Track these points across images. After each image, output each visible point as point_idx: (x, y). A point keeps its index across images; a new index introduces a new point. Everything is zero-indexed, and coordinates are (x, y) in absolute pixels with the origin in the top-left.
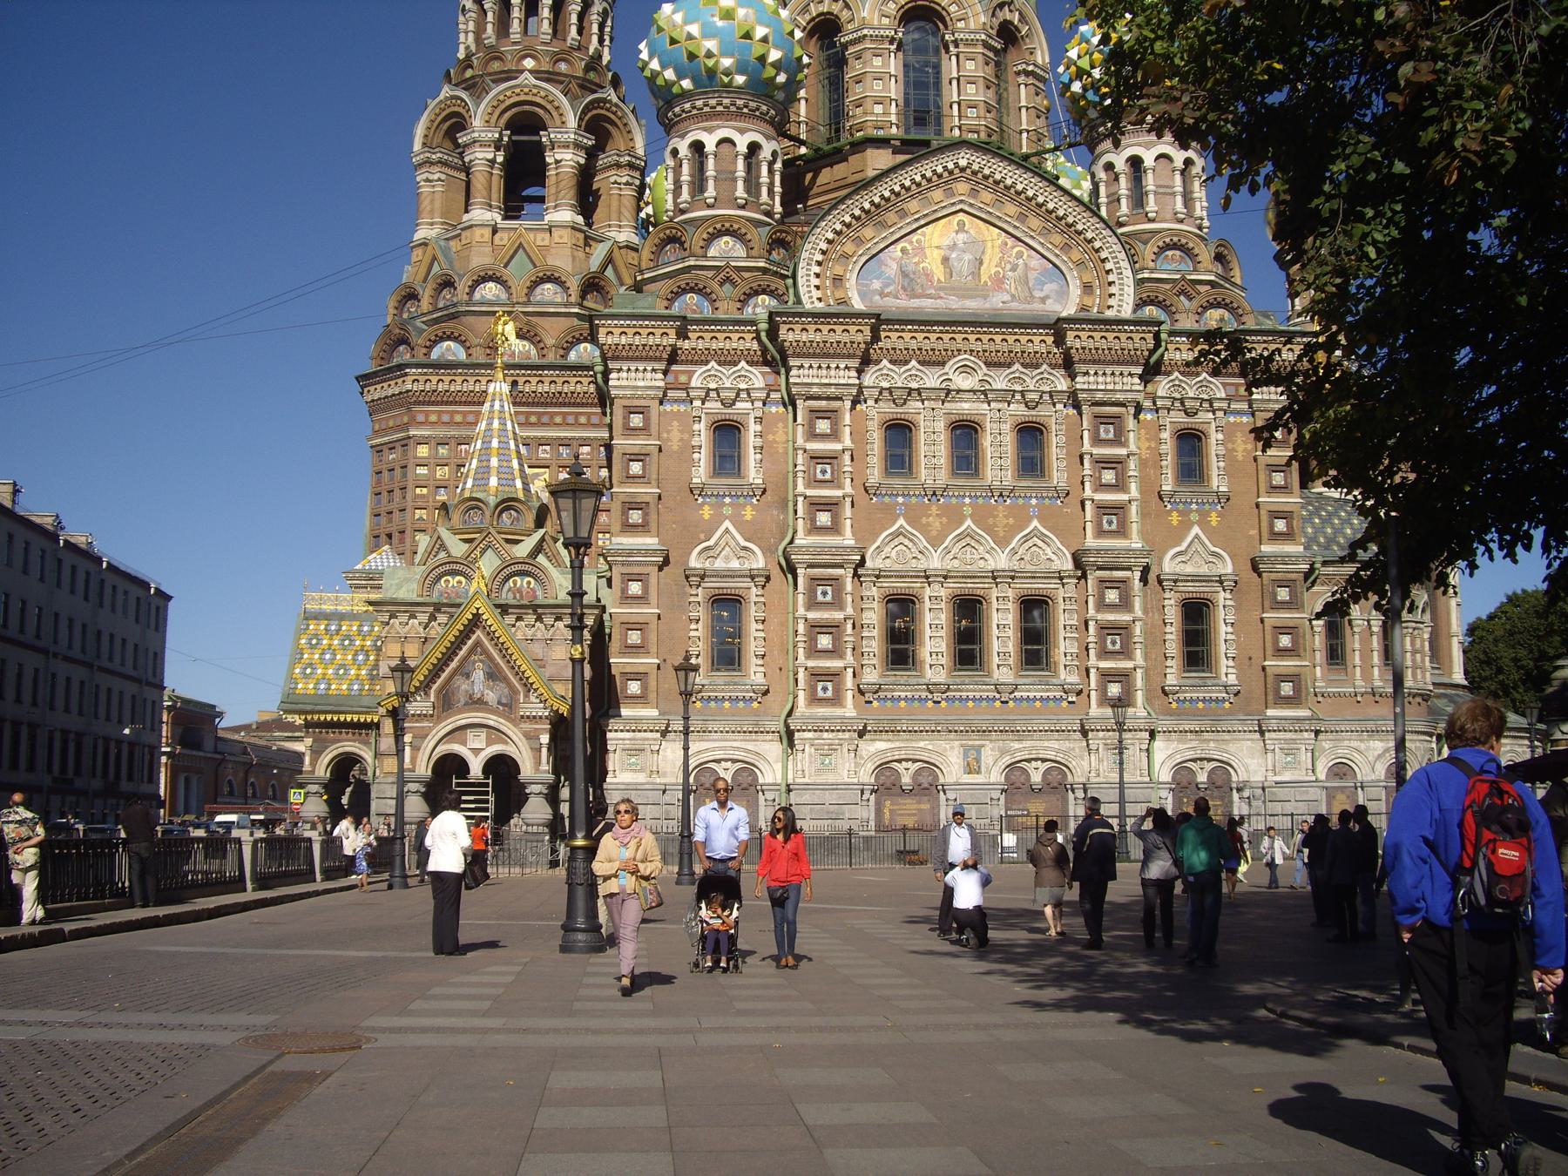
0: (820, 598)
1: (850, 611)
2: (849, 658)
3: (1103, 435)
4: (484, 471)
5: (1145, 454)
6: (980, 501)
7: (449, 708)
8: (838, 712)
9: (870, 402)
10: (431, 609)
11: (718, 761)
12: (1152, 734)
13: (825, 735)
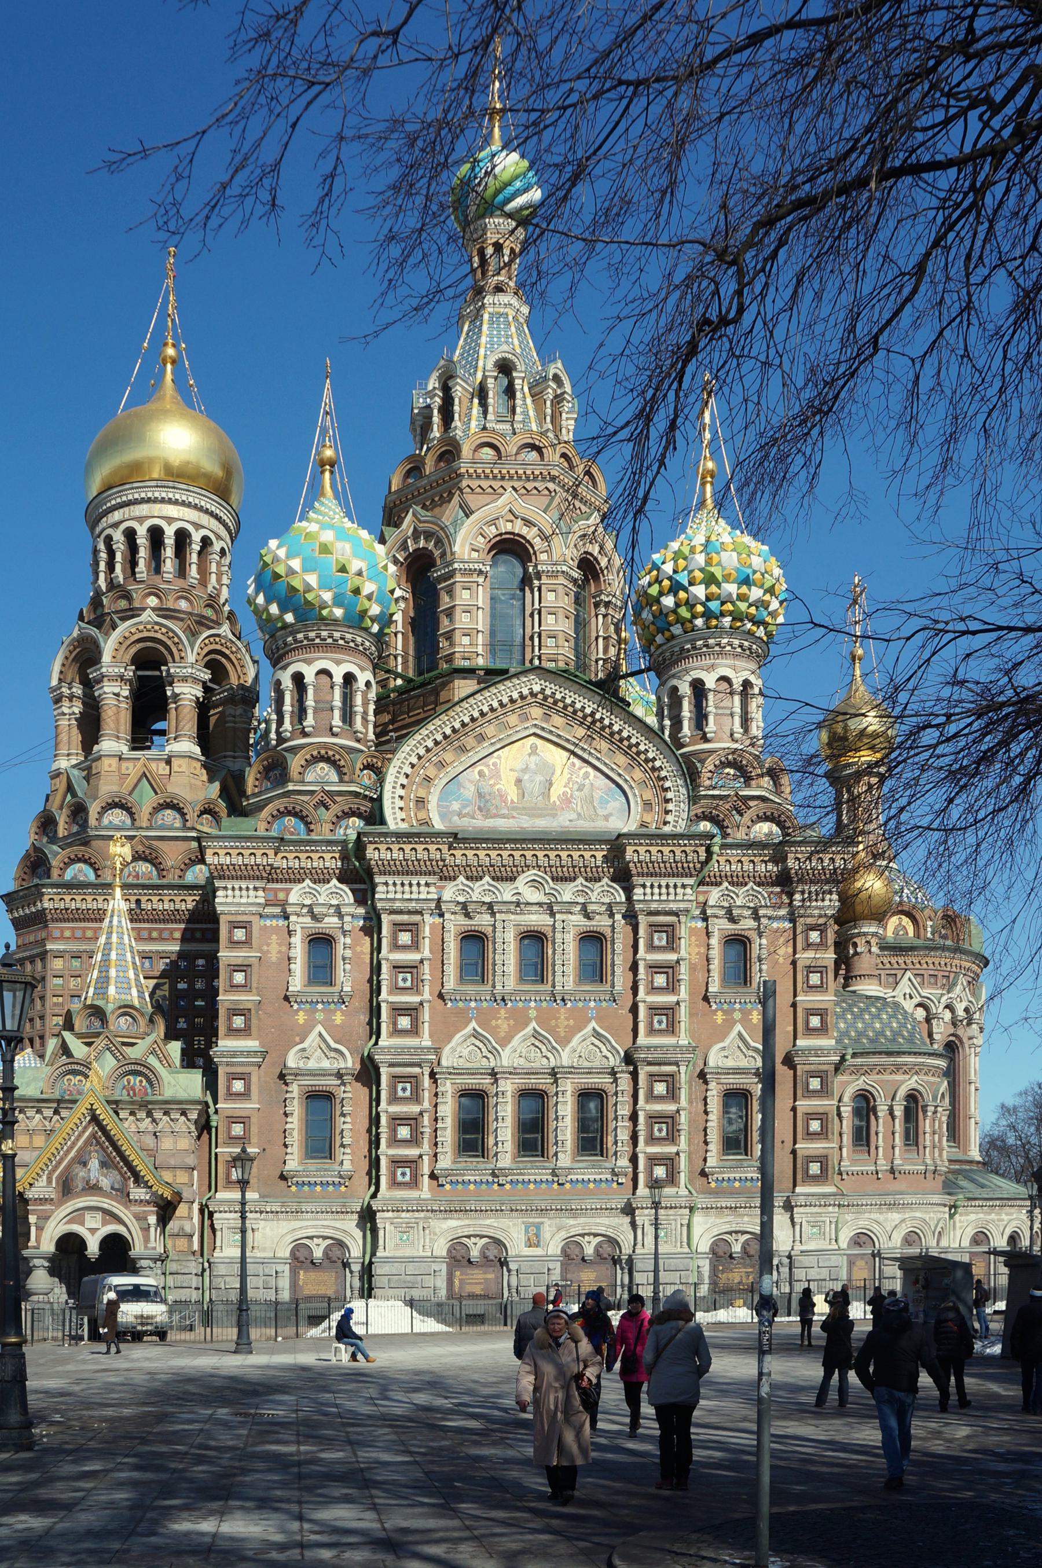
0: (400, 1093)
1: (426, 1104)
2: (426, 1147)
3: (656, 943)
4: (104, 981)
5: (695, 959)
6: (544, 1004)
7: (69, 1193)
8: (413, 1194)
9: (447, 916)
10: (55, 1105)
11: (311, 1238)
12: (691, 1209)
13: (404, 1215)
